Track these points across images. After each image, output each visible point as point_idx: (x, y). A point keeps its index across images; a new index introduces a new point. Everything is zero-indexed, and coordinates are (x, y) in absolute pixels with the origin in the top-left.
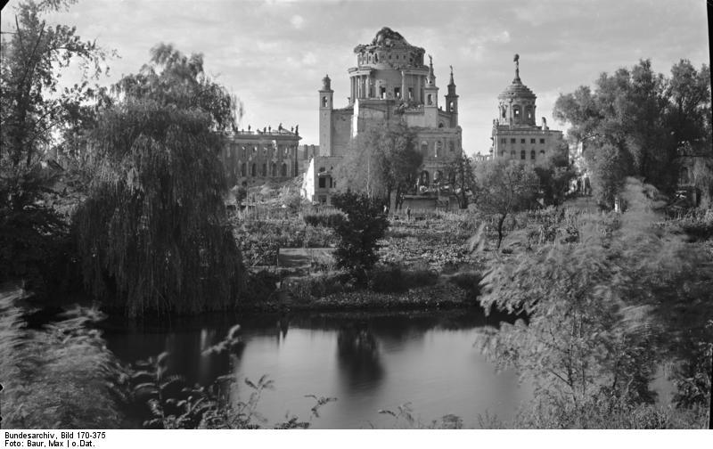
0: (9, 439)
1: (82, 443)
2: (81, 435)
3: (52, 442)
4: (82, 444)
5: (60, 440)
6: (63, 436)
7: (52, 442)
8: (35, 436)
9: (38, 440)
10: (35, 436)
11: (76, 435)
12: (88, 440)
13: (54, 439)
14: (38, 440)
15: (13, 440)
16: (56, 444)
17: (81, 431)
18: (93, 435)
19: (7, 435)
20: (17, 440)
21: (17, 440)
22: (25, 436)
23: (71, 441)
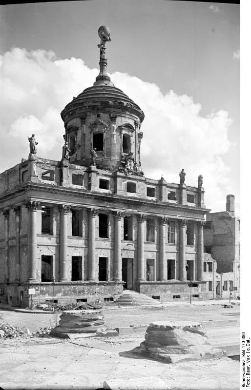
0: (245, 385)
1: (248, 345)
2: (243, 346)
3: (247, 361)
4: (248, 345)
5: (246, 357)
6: (244, 356)
7: (247, 361)
8: (244, 371)
9: (246, 369)
10: (244, 371)
11: (243, 349)
12: (246, 342)
13: (245, 360)
14: (246, 369)
15: (246, 383)
16: (248, 359)
17: (241, 346)
18: (243, 339)
19: (243, 386)
20: (246, 381)
21: (246, 381)
22: (244, 376)
23: (246, 351)
